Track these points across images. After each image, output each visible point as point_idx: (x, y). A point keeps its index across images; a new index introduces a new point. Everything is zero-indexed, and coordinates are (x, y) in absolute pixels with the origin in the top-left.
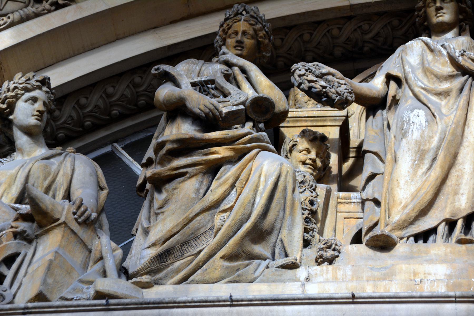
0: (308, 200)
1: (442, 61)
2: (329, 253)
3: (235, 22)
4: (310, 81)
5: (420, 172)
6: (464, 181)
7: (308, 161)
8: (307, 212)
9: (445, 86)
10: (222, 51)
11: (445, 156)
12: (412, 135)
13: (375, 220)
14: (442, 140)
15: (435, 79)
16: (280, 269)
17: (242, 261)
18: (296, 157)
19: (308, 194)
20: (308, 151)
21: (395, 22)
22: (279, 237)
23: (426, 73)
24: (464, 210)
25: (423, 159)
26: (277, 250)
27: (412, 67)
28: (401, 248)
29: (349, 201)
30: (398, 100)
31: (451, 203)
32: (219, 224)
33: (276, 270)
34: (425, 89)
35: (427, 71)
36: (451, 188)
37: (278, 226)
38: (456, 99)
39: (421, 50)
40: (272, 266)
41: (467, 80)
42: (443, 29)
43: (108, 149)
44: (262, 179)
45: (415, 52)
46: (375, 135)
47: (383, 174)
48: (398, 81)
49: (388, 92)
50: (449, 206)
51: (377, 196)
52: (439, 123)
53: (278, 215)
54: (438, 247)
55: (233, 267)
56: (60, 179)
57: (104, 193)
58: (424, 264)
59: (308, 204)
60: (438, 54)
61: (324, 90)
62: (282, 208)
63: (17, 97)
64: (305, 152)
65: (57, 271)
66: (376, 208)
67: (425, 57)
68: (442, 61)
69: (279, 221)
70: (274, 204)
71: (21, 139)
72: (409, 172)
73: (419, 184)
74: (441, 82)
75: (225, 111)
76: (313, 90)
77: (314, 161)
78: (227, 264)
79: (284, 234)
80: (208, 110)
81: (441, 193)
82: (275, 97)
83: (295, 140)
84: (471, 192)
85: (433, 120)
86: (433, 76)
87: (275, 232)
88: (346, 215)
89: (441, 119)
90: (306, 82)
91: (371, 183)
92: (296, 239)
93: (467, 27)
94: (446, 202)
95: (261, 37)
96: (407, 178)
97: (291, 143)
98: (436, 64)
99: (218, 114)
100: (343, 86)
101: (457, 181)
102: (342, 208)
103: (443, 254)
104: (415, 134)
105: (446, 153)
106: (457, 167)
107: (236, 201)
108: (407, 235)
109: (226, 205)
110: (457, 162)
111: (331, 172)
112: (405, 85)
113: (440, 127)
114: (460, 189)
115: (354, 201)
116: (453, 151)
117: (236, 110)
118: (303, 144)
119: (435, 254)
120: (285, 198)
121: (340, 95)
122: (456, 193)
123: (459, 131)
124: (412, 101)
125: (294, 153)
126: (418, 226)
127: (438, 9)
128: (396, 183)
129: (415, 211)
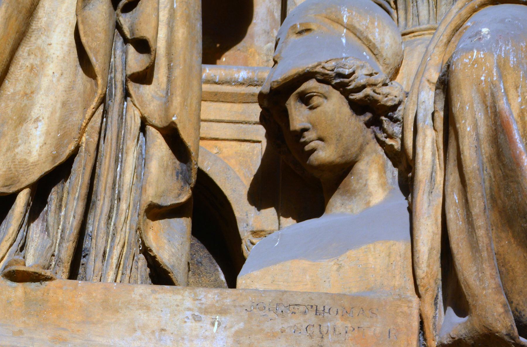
6: (45, 82)
24: (35, 164)
31: (8, 150)
36: (12, 104)
84: (58, 115)
101: (29, 82)
105: (10, 11)
106: (33, 39)
110: (34, 26)
114: (33, 105)
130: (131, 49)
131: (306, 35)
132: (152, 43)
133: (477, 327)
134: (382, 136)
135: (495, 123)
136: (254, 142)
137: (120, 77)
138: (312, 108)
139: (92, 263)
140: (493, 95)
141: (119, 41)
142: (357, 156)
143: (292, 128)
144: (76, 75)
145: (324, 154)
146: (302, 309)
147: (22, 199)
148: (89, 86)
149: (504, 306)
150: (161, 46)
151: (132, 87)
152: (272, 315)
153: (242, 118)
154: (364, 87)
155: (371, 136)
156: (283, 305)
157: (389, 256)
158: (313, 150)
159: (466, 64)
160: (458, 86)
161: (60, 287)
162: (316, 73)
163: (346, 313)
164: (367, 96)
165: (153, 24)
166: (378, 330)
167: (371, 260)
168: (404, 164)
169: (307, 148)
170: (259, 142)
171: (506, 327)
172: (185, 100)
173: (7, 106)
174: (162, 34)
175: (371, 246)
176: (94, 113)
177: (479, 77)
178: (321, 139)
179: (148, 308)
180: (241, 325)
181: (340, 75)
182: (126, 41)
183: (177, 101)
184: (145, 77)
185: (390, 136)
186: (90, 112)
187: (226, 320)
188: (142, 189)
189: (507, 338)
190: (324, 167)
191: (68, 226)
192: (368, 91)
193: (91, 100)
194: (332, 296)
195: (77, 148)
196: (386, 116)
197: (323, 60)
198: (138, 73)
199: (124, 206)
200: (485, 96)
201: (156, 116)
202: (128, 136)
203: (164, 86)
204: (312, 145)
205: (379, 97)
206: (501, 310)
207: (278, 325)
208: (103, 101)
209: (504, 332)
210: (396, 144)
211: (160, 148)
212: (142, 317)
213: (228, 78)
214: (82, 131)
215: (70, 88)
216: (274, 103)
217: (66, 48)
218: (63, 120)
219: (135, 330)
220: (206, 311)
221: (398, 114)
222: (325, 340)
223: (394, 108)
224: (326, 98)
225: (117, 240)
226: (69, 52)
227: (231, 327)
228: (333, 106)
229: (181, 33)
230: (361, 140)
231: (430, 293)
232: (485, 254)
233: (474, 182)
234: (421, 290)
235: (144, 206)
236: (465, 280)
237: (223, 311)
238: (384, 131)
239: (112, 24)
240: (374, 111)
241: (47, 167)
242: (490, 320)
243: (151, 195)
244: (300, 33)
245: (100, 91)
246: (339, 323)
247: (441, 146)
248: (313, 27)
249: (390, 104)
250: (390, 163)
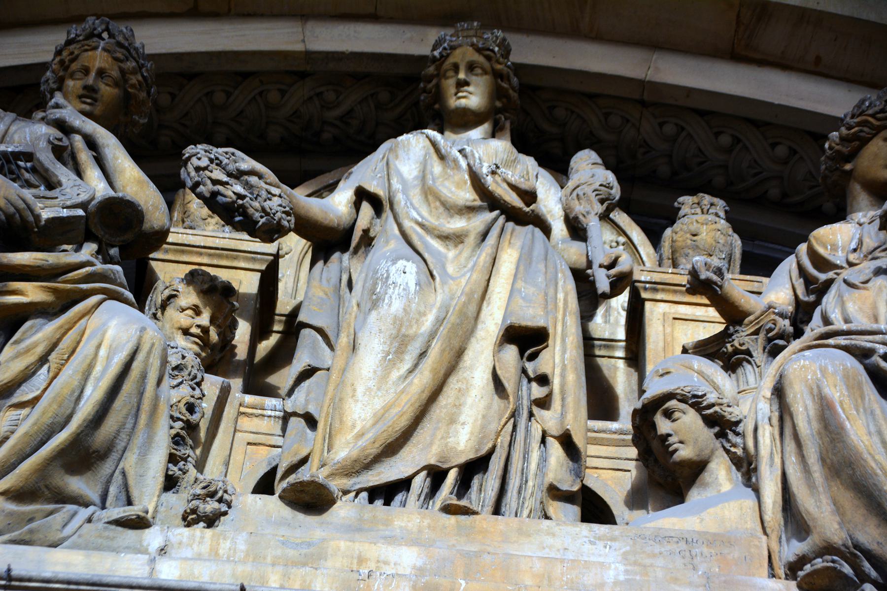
0: (184, 402)
1: (456, 178)
2: (211, 506)
3: (86, 50)
4: (215, 182)
5: (395, 374)
6: (469, 401)
7: (194, 330)
8: (179, 424)
9: (457, 224)
10: (53, 101)
11: (443, 351)
12: (390, 305)
13: (304, 453)
14: (440, 321)
15: (441, 209)
16: (113, 527)
17: (42, 504)
18: (171, 320)
19: (185, 391)
20: (197, 311)
21: (384, 96)
22: (120, 467)
23: (426, 197)
24: (462, 452)
25: (402, 353)
26: (113, 490)
27: (403, 181)
28: (344, 510)
29: (260, 412)
30: (373, 239)
32: (6, 429)
33: (105, 528)
34: (422, 225)
35: (429, 193)
36: (444, 411)
37: (120, 445)
38: (473, 251)
39: (423, 152)
40: (99, 520)
41: (495, 220)
42: (465, 120)
44: (103, 352)
45: (411, 155)
46: (324, 296)
47: (328, 369)
48: (377, 204)
49: (356, 220)
50: (437, 442)
51: (312, 409)
52: (439, 291)
53: (124, 424)
54: (408, 515)
55: (23, 513)
58: (379, 545)
59: (184, 410)
60: (452, 164)
61: (240, 202)
62: (133, 411)
64: (189, 312)
66: (308, 431)
67: (429, 167)
68: (456, 178)
69: (123, 436)
70: (118, 404)
72: (375, 372)
73: (390, 397)
74: (452, 216)
75: (46, 215)
76: (219, 198)
77: (205, 330)
78: (12, 507)
79: (130, 462)
80: (12, 210)
81: (428, 417)
82: (146, 202)
83: (175, 287)
84: (479, 422)
85: (430, 283)
86: (438, 204)
87: (114, 456)
88: (252, 438)
89: (443, 283)
90: (209, 182)
91: (306, 384)
92: (151, 473)
93: (508, 125)
94: (433, 435)
95: (133, 86)
96: (371, 384)
97: (167, 293)
98: (447, 183)
99: (31, 219)
100: (276, 198)
101: (458, 398)
102: (245, 423)
103: (415, 530)
104: (394, 305)
105: (444, 346)
106: (460, 373)
107: (45, 389)
108: (358, 487)
109: (25, 393)
110: (461, 365)
111: (235, 355)
112: (387, 213)
113: (440, 298)
114: (460, 413)
115: (269, 413)
116: (456, 344)
117: (68, 217)
118: (189, 297)
119: (401, 527)
120: (141, 394)
121: (267, 214)
122: (452, 420)
123: (472, 308)
124: (395, 243)
125: (170, 311)
126: (379, 474)
127: (462, 84)
128: (349, 390)
129: (377, 445)
130: (534, 385)
131: (666, 377)
132: (550, 377)
133: (817, 542)
134: (727, 446)
135: (822, 405)
136: (626, 471)
137: (526, 403)
138: (674, 421)
140: (818, 387)
141: (525, 381)
142: (709, 457)
143: (659, 433)
144: (492, 400)
145: (684, 453)
146: (675, 540)
147: (452, 475)
148: (503, 405)
149: (839, 524)
150: (556, 382)
151: (536, 410)
152: (651, 542)
153: (616, 456)
154: (713, 405)
155: (718, 445)
157: (741, 509)
158: (676, 450)
159: (795, 369)
160: (791, 383)
161: (485, 520)
162: (677, 394)
163: (710, 544)
164: (716, 412)
165: (551, 365)
166: (736, 556)
167: (727, 513)
168: (746, 466)
169: (671, 449)
170: (629, 471)
171: (842, 539)
172: (575, 418)
173: (441, 412)
174: (557, 371)
175: (726, 504)
176: (506, 424)
177: (806, 377)
178: (681, 442)
179: (554, 535)
180: (628, 548)
181: (695, 396)
182: (530, 380)
183: (570, 416)
184: (544, 403)
185: (734, 446)
186: (504, 420)
187: (616, 545)
188: (544, 475)
189: (843, 548)
190: (684, 463)
191: (488, 497)
192: (716, 408)
193: (505, 414)
194: (699, 533)
195: (494, 448)
196: (731, 430)
197: (682, 385)
198: (540, 399)
199: (530, 483)
200: (812, 389)
201: (554, 429)
202: (533, 440)
203: (559, 411)
204: (675, 446)
205: (726, 414)
206: (836, 526)
207: (657, 549)
208: (514, 415)
209: (840, 542)
210: (739, 452)
211: (556, 450)
212: (550, 540)
213: (604, 428)
214: (498, 434)
215: (489, 407)
217: (485, 381)
218: (483, 427)
219: (544, 548)
220: (600, 539)
221: (740, 429)
222: (695, 560)
223: (737, 423)
224: (684, 413)
225: (526, 505)
226: (487, 384)
227: (620, 549)
228: (690, 419)
229: (571, 377)
230: (712, 446)
231: (775, 533)
232: (821, 489)
233: (809, 443)
234: (768, 531)
235: (546, 485)
236: (806, 510)
237: (613, 539)
238: (728, 441)
239: (520, 371)
240: (721, 425)
241: (472, 456)
242: (829, 534)
244: (662, 375)
245: (511, 406)
246: (705, 550)
247: (777, 437)
248: (672, 370)
249: (733, 420)
250: (734, 468)
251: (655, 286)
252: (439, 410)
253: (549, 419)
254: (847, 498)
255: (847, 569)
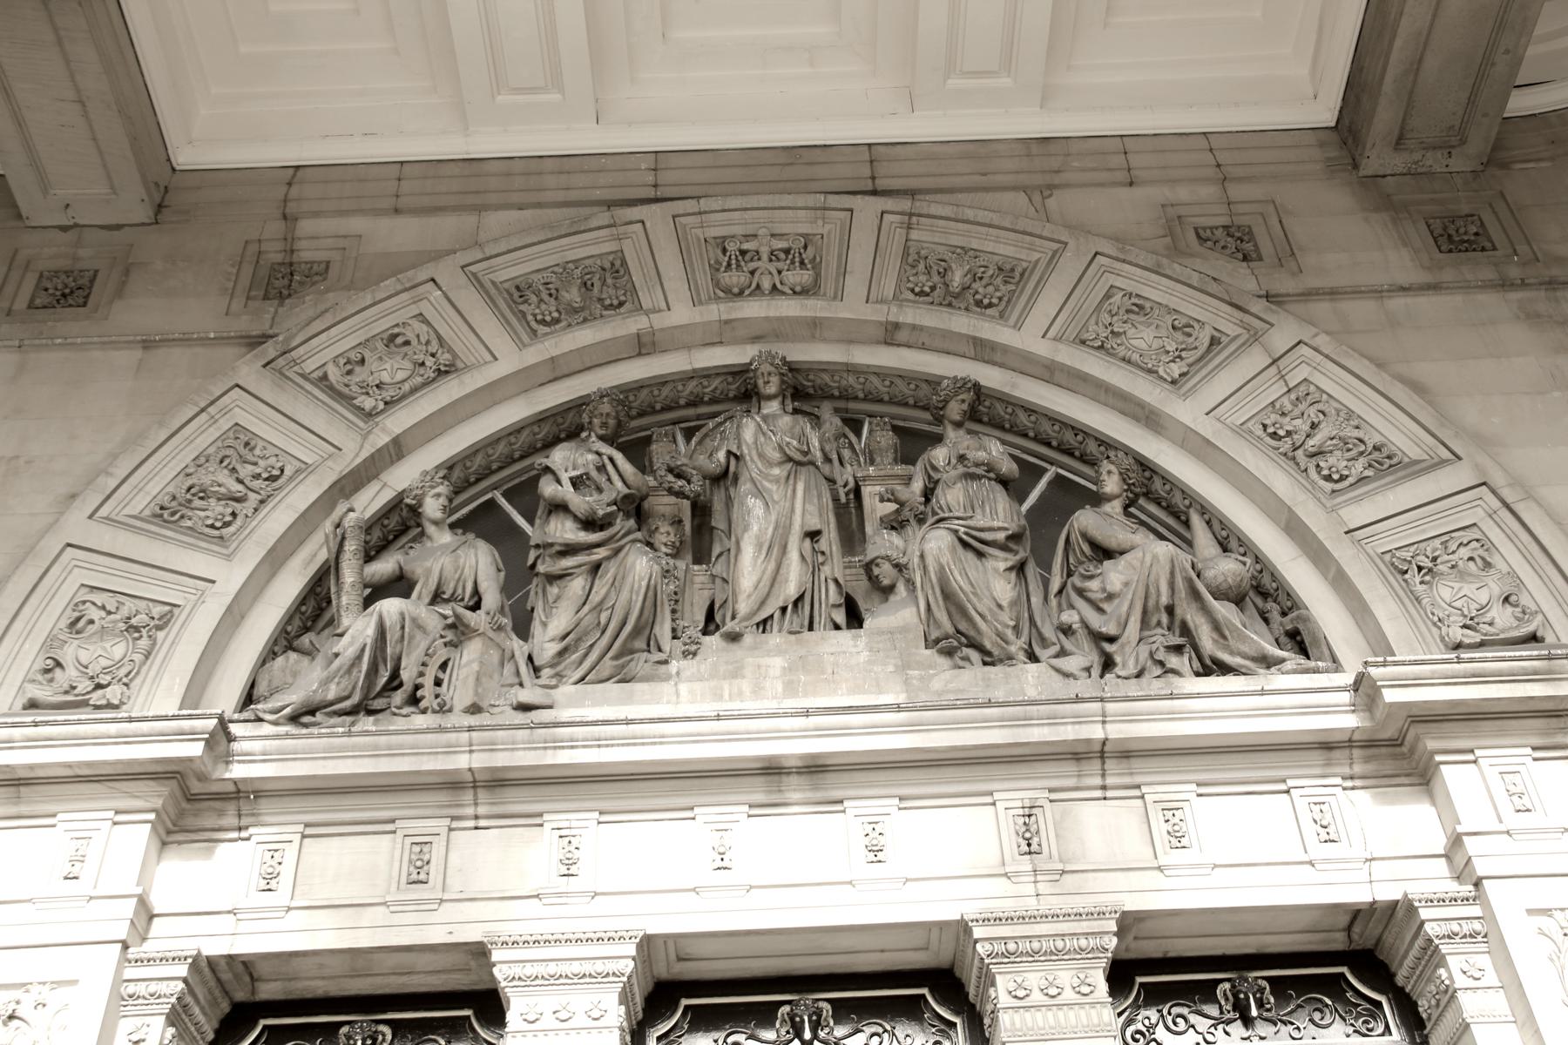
2: (693, 648)
9: (776, 471)
14: (775, 529)
28: (748, 639)
35: (761, 456)
42: (770, 398)
43: (489, 496)
54: (775, 638)
56: (466, 570)
57: (502, 574)
63: (424, 495)
65: (484, 680)
71: (431, 529)
75: (601, 513)
79: (657, 629)
113: (773, 518)
124: (749, 485)
139: (816, 625)
145: (886, 582)
156: (880, 632)
211: (832, 587)
216: (868, 567)
240: (899, 567)
243: (831, 601)
251: (865, 479)
252: (779, 578)
253: (826, 570)
254: (953, 609)
255: (956, 644)
